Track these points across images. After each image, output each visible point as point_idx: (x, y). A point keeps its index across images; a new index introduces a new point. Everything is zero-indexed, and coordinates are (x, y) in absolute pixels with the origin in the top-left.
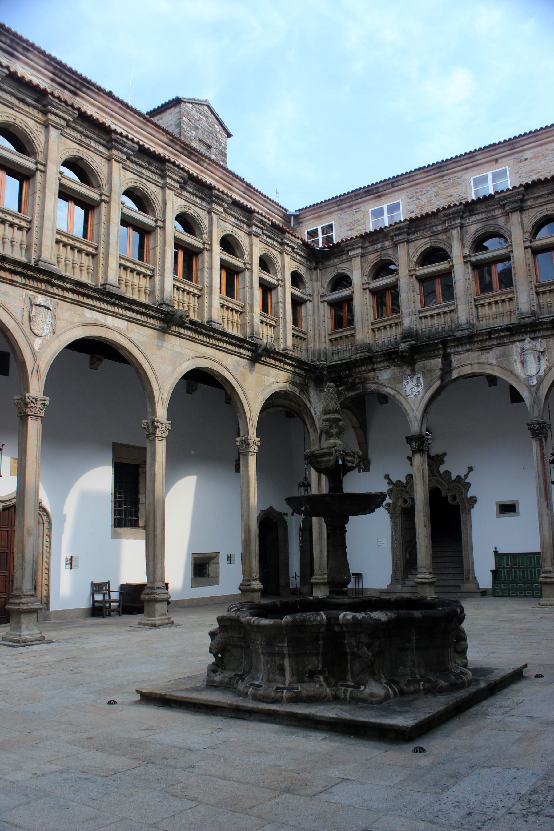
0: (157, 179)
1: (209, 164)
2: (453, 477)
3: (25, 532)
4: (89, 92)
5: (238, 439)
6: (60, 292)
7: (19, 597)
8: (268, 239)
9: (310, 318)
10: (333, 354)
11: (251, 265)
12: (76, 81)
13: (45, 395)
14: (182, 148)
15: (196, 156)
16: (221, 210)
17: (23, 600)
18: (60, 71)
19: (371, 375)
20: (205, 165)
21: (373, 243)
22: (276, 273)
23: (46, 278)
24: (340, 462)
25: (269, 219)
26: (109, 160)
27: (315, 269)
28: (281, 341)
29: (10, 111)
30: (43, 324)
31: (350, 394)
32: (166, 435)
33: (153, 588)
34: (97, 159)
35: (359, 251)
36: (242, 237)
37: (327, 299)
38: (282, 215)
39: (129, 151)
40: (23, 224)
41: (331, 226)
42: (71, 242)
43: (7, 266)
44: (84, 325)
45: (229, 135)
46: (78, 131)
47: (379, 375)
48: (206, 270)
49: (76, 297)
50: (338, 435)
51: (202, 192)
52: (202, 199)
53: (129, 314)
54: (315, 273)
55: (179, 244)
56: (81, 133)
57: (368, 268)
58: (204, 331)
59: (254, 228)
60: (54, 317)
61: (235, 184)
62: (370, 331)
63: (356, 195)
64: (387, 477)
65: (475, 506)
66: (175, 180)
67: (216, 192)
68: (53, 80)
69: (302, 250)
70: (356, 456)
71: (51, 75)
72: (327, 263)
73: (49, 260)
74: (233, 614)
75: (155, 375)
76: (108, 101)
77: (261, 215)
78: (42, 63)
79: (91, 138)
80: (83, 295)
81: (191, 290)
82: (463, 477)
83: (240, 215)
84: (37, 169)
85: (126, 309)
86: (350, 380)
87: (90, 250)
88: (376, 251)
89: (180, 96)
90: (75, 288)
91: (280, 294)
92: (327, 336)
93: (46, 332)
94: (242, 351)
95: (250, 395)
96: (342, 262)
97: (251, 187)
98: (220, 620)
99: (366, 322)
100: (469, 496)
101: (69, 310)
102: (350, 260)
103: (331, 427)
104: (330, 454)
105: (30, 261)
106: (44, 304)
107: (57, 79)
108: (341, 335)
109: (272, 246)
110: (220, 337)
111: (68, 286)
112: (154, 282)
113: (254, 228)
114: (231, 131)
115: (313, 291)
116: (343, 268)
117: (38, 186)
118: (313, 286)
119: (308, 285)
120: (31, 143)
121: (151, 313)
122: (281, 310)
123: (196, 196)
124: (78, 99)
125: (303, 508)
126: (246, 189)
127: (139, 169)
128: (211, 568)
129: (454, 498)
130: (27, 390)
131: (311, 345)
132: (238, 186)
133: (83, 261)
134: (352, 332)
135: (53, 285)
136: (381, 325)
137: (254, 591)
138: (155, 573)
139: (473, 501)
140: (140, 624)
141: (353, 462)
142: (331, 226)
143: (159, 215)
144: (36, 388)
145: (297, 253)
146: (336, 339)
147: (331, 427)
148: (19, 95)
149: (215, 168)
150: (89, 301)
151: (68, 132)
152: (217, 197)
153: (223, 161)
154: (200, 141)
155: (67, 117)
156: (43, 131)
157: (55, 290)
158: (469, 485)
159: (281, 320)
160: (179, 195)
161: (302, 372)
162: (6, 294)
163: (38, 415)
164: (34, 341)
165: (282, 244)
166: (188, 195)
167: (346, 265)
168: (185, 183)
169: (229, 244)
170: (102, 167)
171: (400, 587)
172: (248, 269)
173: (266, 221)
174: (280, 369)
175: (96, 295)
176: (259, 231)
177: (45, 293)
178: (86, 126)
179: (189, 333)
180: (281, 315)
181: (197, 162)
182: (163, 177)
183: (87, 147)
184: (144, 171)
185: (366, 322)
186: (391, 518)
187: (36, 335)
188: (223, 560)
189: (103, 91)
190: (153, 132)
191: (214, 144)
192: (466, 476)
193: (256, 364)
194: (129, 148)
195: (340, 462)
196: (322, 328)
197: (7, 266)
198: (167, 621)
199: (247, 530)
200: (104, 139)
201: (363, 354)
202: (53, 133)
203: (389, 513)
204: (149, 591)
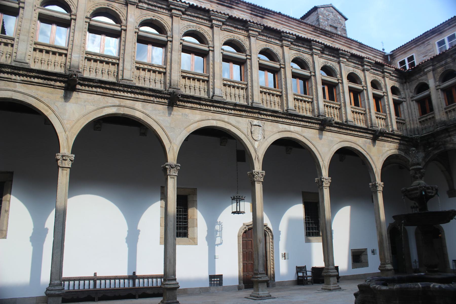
0: (308, 51)
1: (336, 37)
3: (258, 241)
4: (269, 15)
5: (370, 184)
6: (265, 117)
7: (257, 274)
8: (374, 71)
9: (406, 111)
10: (423, 130)
11: (367, 87)
12: (262, 11)
13: (262, 170)
14: (321, 32)
15: (329, 34)
16: (345, 60)
17: (259, 276)
18: (254, 9)
19: (448, 139)
20: (335, 38)
21: (439, 61)
22: (382, 89)
23: (257, 111)
24: (424, 193)
25: (373, 60)
26: (282, 46)
27: (405, 83)
28: (390, 126)
30: (258, 134)
31: (436, 152)
32: (329, 185)
33: (328, 269)
34: (276, 47)
35: (431, 68)
36: (359, 73)
37: (415, 99)
38: (382, 56)
39: (291, 40)
40: (243, 86)
41: (412, 57)
42: (268, 91)
43: (238, 108)
44: (279, 132)
45: (346, 19)
46: (265, 36)
47: (453, 138)
48: (341, 94)
49: (273, 118)
50: (421, 178)
51: (333, 53)
52: (334, 56)
53: (302, 123)
54: (405, 85)
55: (324, 83)
56: (266, 36)
57: (438, 77)
58: (344, 127)
59: (365, 67)
60: (264, 130)
61: (353, 44)
62: (445, 114)
63: (426, 36)
66: (318, 50)
67: (341, 51)
68: (251, 14)
69: (395, 74)
70: (434, 189)
71: (250, 12)
72: (412, 78)
73: (258, 102)
74: (366, 283)
75: (320, 154)
76: (279, 17)
77: (369, 58)
78: (246, 8)
79: (272, 38)
80: (277, 117)
81: (334, 106)
83: (356, 61)
84: (247, 58)
85: (300, 121)
86: (435, 143)
87: (278, 93)
88: (442, 66)
89: (316, 5)
91: (386, 100)
92: (417, 120)
93: (260, 138)
94: (367, 135)
95: (375, 158)
96: (421, 76)
97: (362, 44)
98: (360, 287)
99: (441, 109)
102: (426, 74)
103: (416, 173)
104: (416, 189)
105: (248, 104)
106: (257, 124)
107: (253, 13)
108: (426, 118)
109: (377, 75)
110: (353, 129)
111: (269, 113)
112: (314, 104)
113: (365, 67)
114: (347, 17)
115: (406, 96)
116: (422, 79)
117: (249, 67)
118: (405, 93)
119: (402, 93)
120: (243, 46)
121: (314, 121)
122: (387, 109)
123: (331, 56)
124: (264, 20)
125: (403, 222)
126: (360, 46)
127: (298, 48)
128: (363, 257)
130: (253, 168)
131: (408, 126)
132: (355, 45)
133: (275, 100)
134: (433, 115)
135: (261, 114)
136: (451, 108)
137: (388, 270)
138: (328, 261)
140: (322, 289)
141: (432, 193)
142: (412, 57)
143: (311, 69)
144: (258, 167)
145: (393, 76)
146: (423, 121)
147: (416, 173)
148: (235, 26)
149: (340, 38)
150: (281, 120)
152: (342, 54)
153: (345, 34)
154: (331, 26)
156: (248, 40)
157: (263, 117)
159: (388, 115)
160: (321, 57)
161: (405, 143)
162: (238, 122)
165: (383, 72)
166: (326, 56)
167: (423, 77)
168: (323, 50)
169: (352, 78)
170: (279, 51)
172: (365, 90)
173: (372, 61)
174: (391, 142)
175: (283, 116)
176: (369, 68)
177: (257, 118)
178: (268, 32)
179: (336, 129)
180: (388, 112)
181: (330, 37)
182: (311, 49)
184: (301, 48)
185: (441, 109)
188: (369, 253)
189: (276, 13)
190: (304, 27)
191: (339, 26)
193: (377, 141)
194: (291, 39)
195: (424, 193)
196: (414, 116)
197: (238, 108)
198: (337, 287)
199: (380, 235)
200: (278, 37)
201: (441, 127)
202: (253, 39)
204: (326, 271)
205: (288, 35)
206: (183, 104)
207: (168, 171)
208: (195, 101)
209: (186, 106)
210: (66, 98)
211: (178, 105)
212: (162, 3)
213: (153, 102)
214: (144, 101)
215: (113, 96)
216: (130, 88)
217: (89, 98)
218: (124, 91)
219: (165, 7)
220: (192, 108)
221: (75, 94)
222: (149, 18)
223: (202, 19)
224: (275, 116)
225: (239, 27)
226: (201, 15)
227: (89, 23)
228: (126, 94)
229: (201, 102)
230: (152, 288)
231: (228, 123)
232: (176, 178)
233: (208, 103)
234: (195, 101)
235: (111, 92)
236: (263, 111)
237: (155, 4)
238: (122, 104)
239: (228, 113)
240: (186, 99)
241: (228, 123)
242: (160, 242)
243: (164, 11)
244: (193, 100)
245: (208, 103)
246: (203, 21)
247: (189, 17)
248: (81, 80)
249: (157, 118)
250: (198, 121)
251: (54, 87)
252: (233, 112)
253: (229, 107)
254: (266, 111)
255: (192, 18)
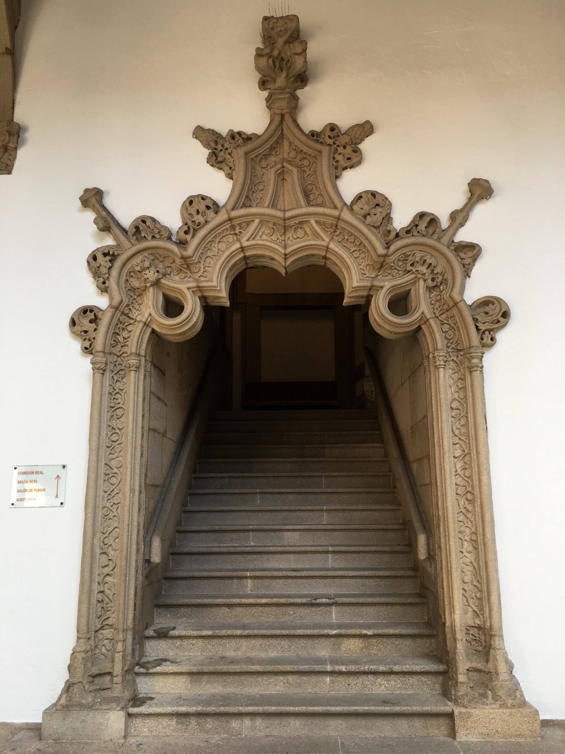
2: (401, 219)
64: (93, 199)
65: (502, 336)
82: (445, 223)
100: (475, 290)
129: (400, 303)
139: (494, 315)
158: (470, 252)
171: (115, 720)
186: (99, 370)
192: (459, 217)
203: (88, 350)
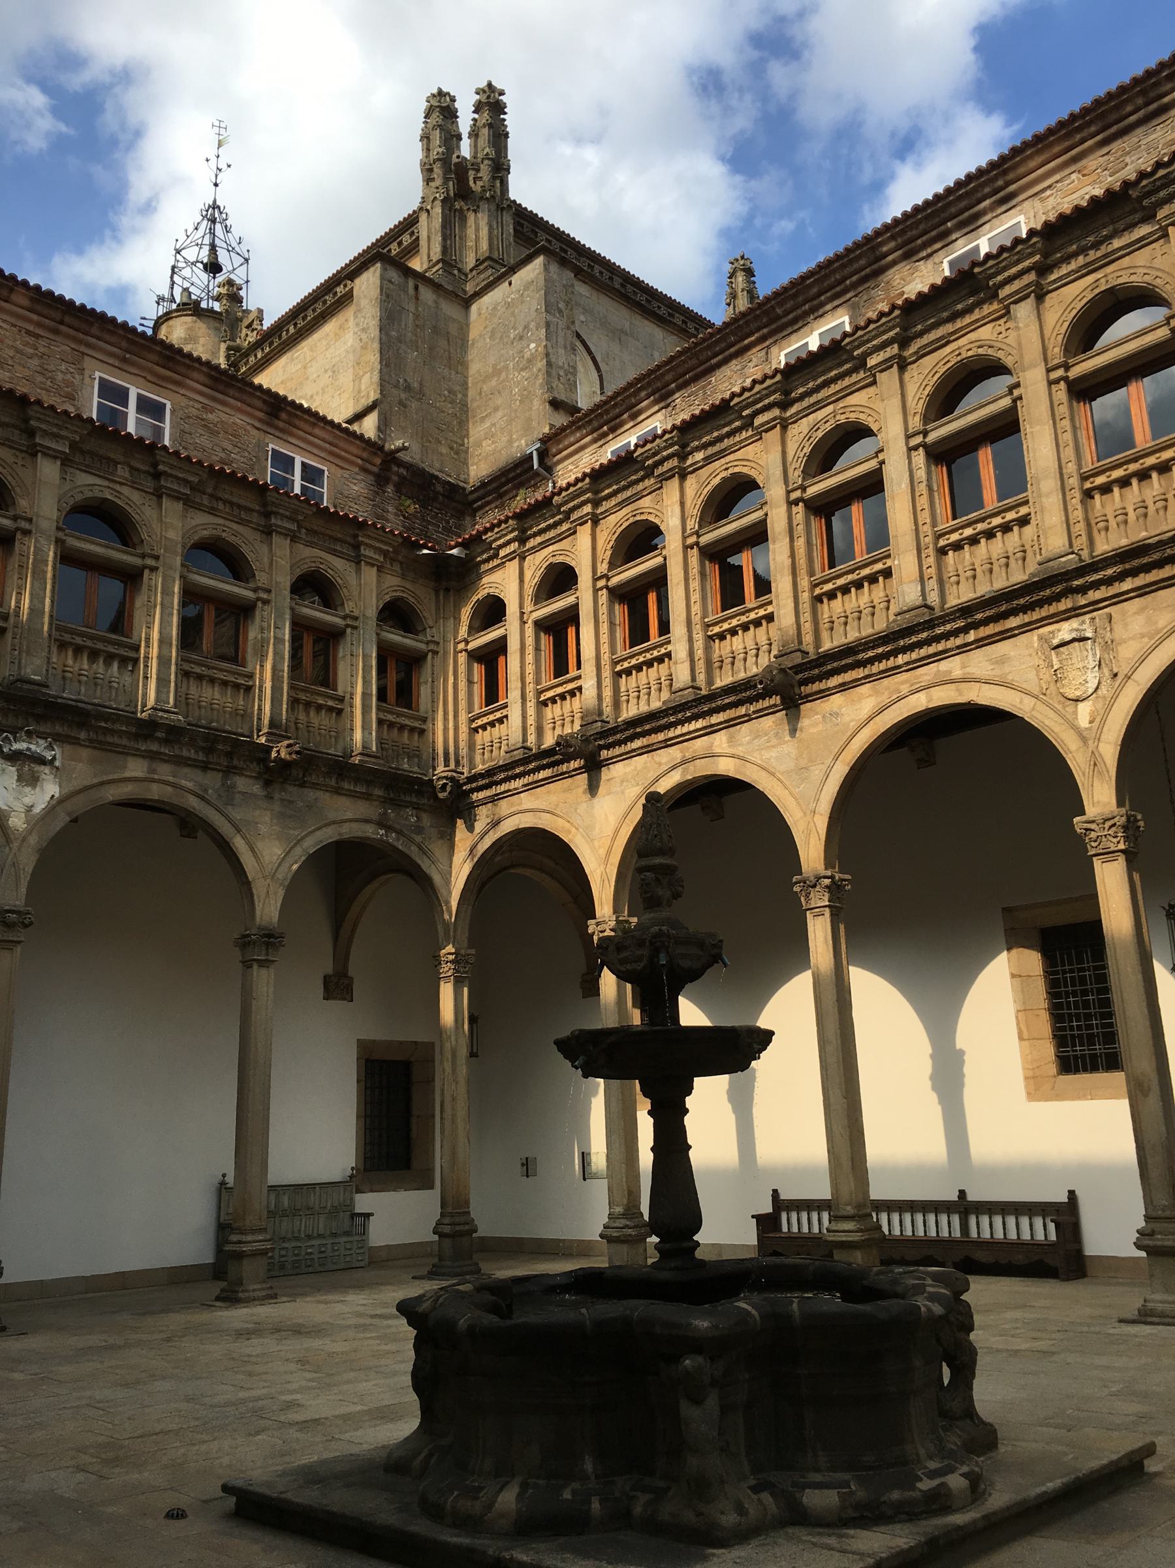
29: (948, 349)
34: (1141, 257)
43: (979, 616)
46: (1075, 255)
56: (1083, 251)
79: (1109, 238)
90: (1127, 566)
101: (1142, 610)
111: (1110, 572)
135: (1083, 590)
144: (1100, 798)
148: (945, 314)
151: (1053, 277)
155: (1027, 263)
157: (1094, 595)
163: (1113, 849)
164: (1075, 713)
183: (1110, 259)
187: (1077, 701)
205: (1161, 172)
206: (816, 686)
207: (802, 899)
208: (843, 662)
209: (828, 689)
210: (593, 788)
211: (807, 696)
212: (727, 420)
213: (748, 718)
214: (729, 724)
215: (666, 744)
216: (688, 709)
217: (628, 770)
218: (682, 722)
219: (737, 424)
220: (844, 687)
221: (605, 774)
222: (717, 480)
223: (841, 377)
224: (1147, 568)
225: (959, 307)
226: (831, 369)
227: (607, 587)
228: (686, 728)
229: (860, 656)
230: (1019, 1245)
231: (965, 680)
232: (827, 911)
233: (880, 650)
234: (843, 662)
235: (661, 736)
236: (1082, 576)
237: (715, 434)
238: (688, 755)
239: (958, 647)
240: (816, 671)
241: (965, 680)
242: (1029, 1094)
243: (744, 435)
244: (835, 665)
245: (880, 650)
246: (847, 381)
247: (806, 403)
248: (600, 739)
249: (770, 756)
250: (870, 719)
251: (569, 775)
252: (972, 636)
253: (948, 627)
254: (1096, 571)
255: (813, 399)
